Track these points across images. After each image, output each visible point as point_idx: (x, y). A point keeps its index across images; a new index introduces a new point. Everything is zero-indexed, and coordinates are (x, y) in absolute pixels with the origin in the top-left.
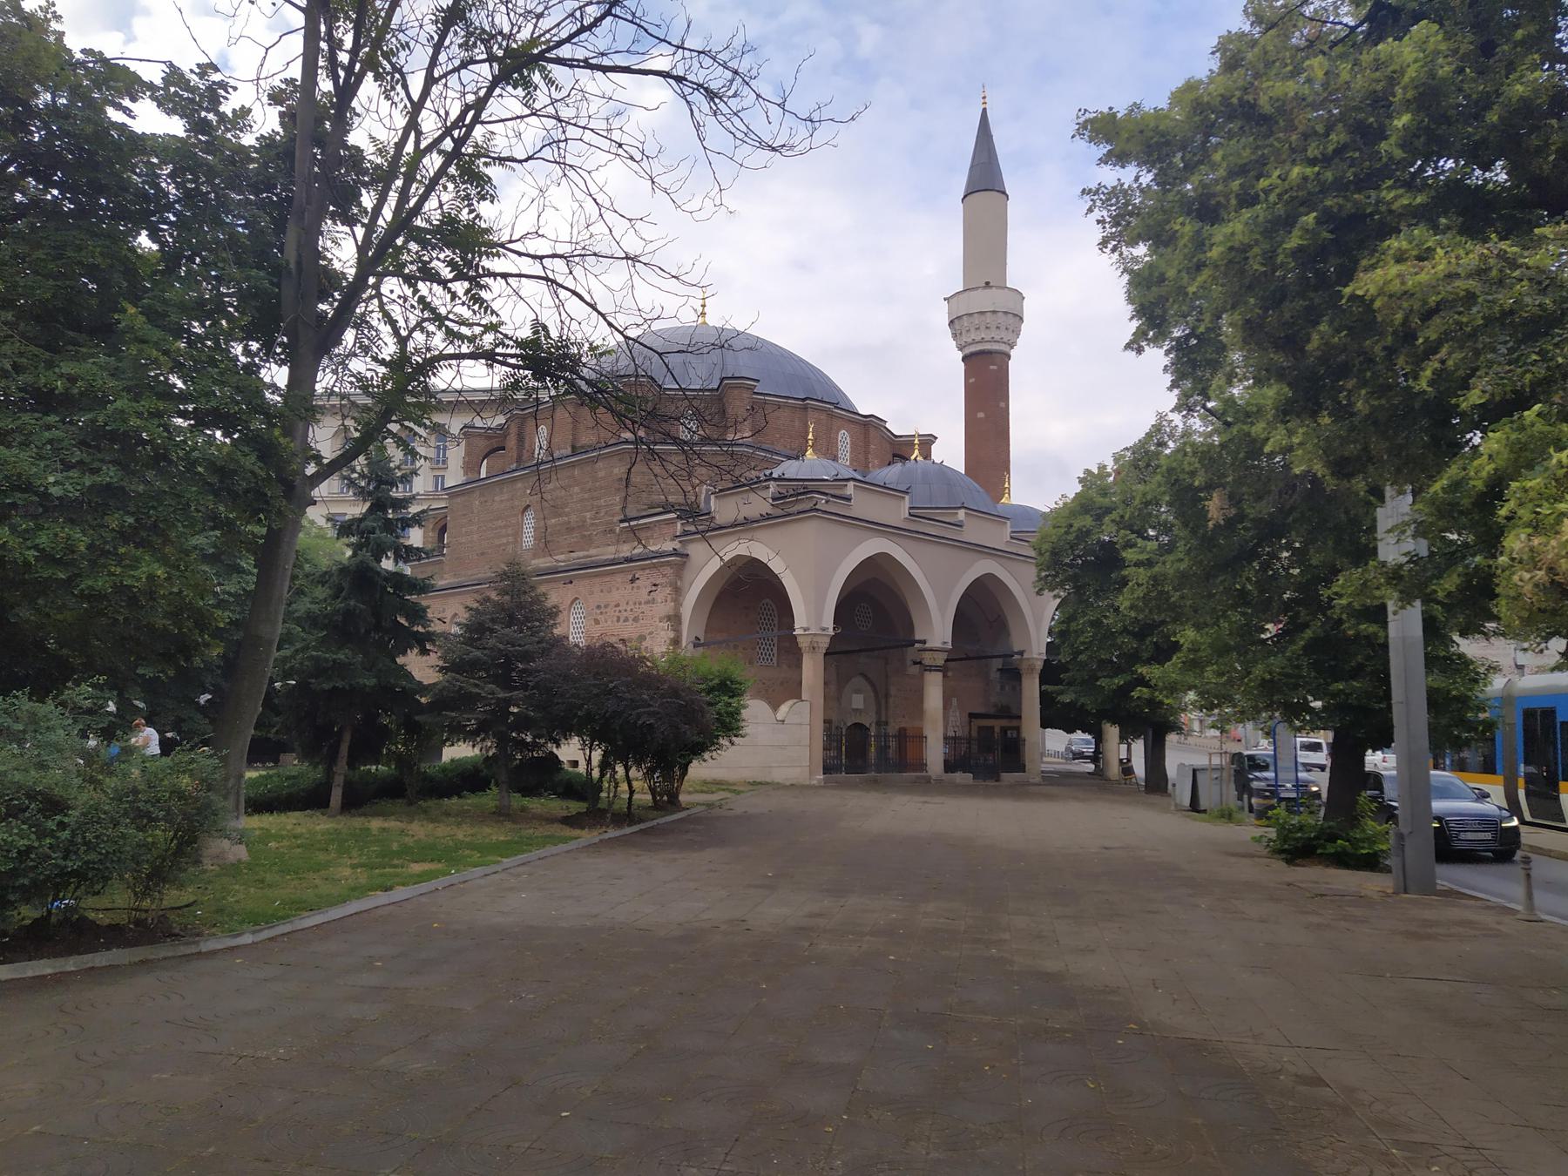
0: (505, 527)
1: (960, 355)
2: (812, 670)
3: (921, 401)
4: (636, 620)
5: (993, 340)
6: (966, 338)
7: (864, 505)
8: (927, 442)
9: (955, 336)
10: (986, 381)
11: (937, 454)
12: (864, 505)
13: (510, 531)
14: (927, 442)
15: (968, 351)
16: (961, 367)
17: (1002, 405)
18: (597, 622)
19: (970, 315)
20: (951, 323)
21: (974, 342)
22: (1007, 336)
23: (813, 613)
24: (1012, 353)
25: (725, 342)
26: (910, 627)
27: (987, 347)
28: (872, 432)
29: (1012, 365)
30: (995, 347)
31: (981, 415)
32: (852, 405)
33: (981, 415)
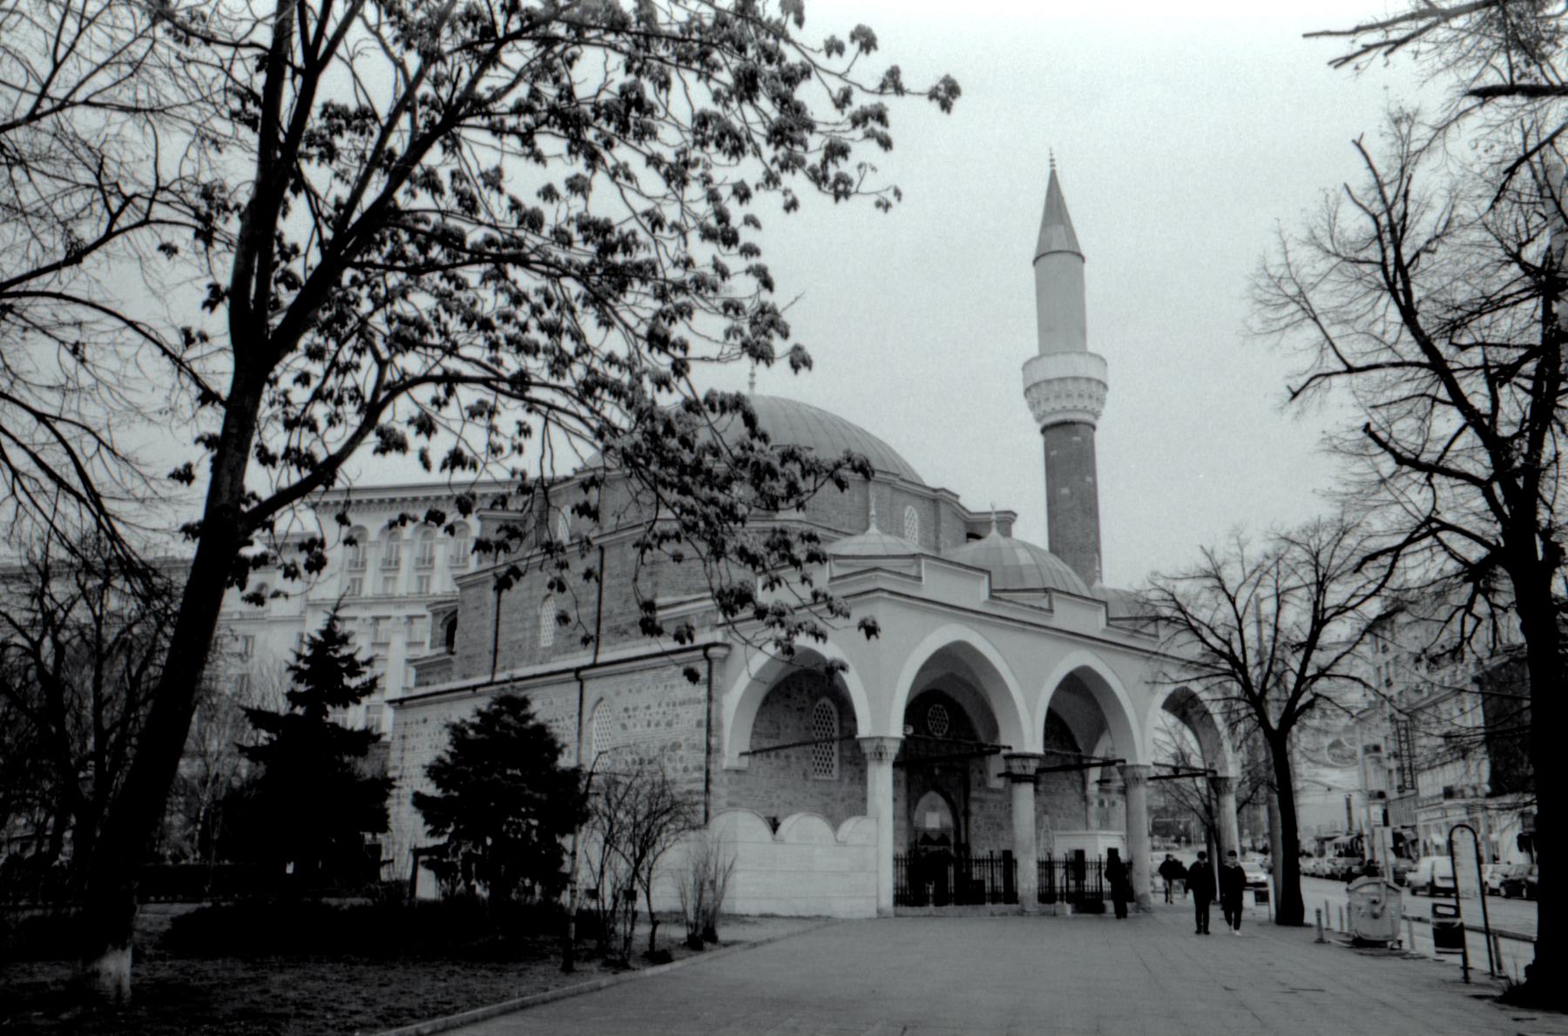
0: (523, 620)
1: (1038, 427)
2: (882, 781)
4: (669, 724)
5: (1075, 409)
6: (1045, 407)
7: (936, 584)
8: (1006, 520)
9: (1032, 407)
11: (1018, 531)
12: (936, 584)
13: (527, 625)
16: (1038, 441)
18: (624, 727)
20: (1027, 391)
21: (1054, 411)
23: (881, 715)
26: (994, 730)
28: (943, 508)
32: (917, 477)
33: (1065, 491)
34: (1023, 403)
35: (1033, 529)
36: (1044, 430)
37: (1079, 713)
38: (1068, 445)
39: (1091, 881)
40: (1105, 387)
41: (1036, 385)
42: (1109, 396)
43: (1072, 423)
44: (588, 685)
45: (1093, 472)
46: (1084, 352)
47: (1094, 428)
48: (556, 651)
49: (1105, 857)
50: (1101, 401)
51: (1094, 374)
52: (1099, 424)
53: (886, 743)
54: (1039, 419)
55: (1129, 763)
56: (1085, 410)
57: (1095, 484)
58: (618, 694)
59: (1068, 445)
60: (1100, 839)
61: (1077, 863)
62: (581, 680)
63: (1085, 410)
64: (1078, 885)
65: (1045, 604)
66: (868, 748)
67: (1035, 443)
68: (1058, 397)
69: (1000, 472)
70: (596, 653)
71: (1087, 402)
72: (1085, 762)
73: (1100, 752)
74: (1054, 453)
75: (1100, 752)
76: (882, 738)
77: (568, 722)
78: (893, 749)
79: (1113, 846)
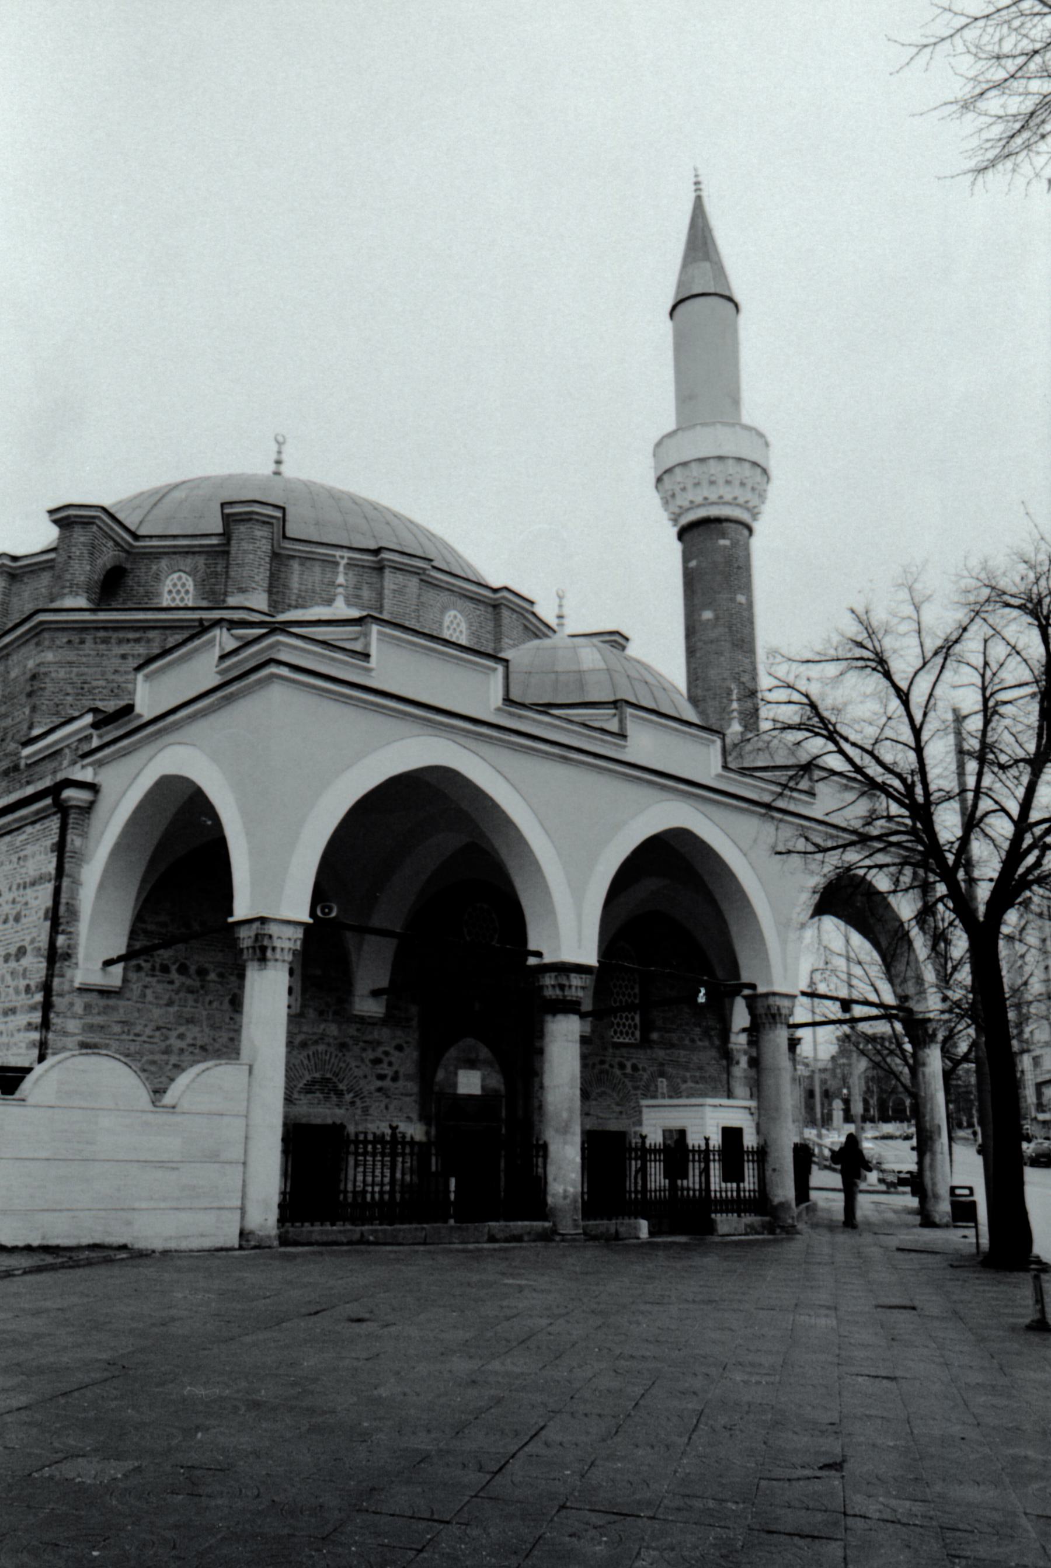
2: (268, 996)
5: (721, 501)
6: (683, 500)
7: (391, 665)
15: (685, 520)
16: (677, 547)
17: (741, 598)
20: (659, 480)
21: (693, 506)
23: (274, 881)
27: (714, 512)
33: (707, 615)
34: (654, 499)
36: (681, 535)
37: (671, 905)
38: (713, 551)
40: (765, 471)
41: (669, 471)
43: (718, 520)
45: (747, 587)
46: (735, 423)
47: (750, 530)
52: (756, 526)
53: (273, 929)
56: (734, 503)
59: (713, 551)
65: (613, 726)
66: (246, 936)
67: (668, 556)
68: (697, 484)
69: (623, 592)
71: (737, 491)
74: (693, 564)
76: (263, 920)
78: (287, 941)
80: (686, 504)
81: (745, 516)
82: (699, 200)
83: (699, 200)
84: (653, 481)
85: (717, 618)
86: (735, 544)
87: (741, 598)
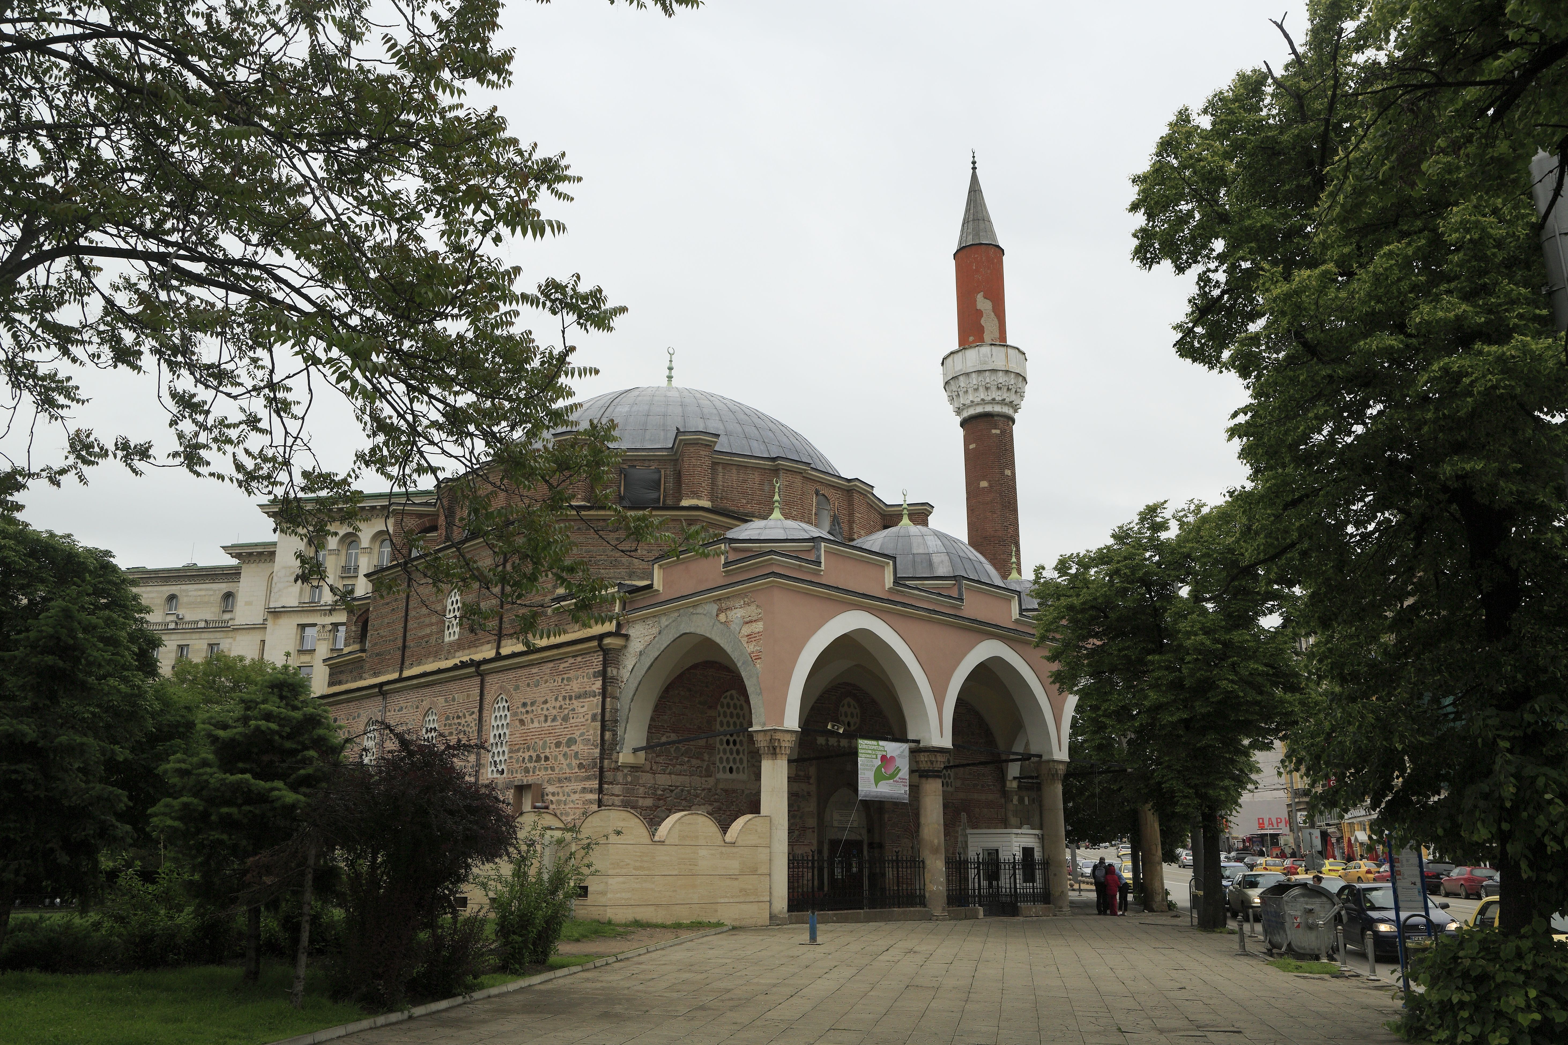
1: (958, 420)
3: (917, 463)
6: (965, 400)
9: (951, 399)
10: (989, 442)
14: (920, 513)
15: (966, 414)
16: (961, 432)
17: (1008, 472)
19: (967, 374)
20: (947, 383)
22: (1010, 397)
24: (1017, 416)
25: (692, 401)
27: (988, 408)
29: (1018, 430)
30: (997, 409)
31: (984, 484)
33: (984, 484)
35: (951, 520)
36: (963, 424)
39: (1005, 881)
42: (1029, 389)
44: (489, 679)
45: (1012, 465)
48: (459, 645)
49: (1019, 856)
50: (1020, 393)
51: (1013, 367)
54: (958, 411)
55: (1045, 758)
56: (1003, 402)
57: (1014, 474)
58: (517, 688)
60: (1014, 839)
61: (992, 864)
62: (482, 675)
63: (1003, 402)
64: (990, 886)
70: (498, 647)
72: (1004, 757)
73: (1019, 748)
75: (1019, 748)
77: (469, 719)
79: (1030, 845)
80: (968, 402)
81: (1010, 412)
82: (974, 178)
83: (974, 178)
84: (942, 385)
85: (991, 486)
86: (1003, 432)
87: (1008, 472)
